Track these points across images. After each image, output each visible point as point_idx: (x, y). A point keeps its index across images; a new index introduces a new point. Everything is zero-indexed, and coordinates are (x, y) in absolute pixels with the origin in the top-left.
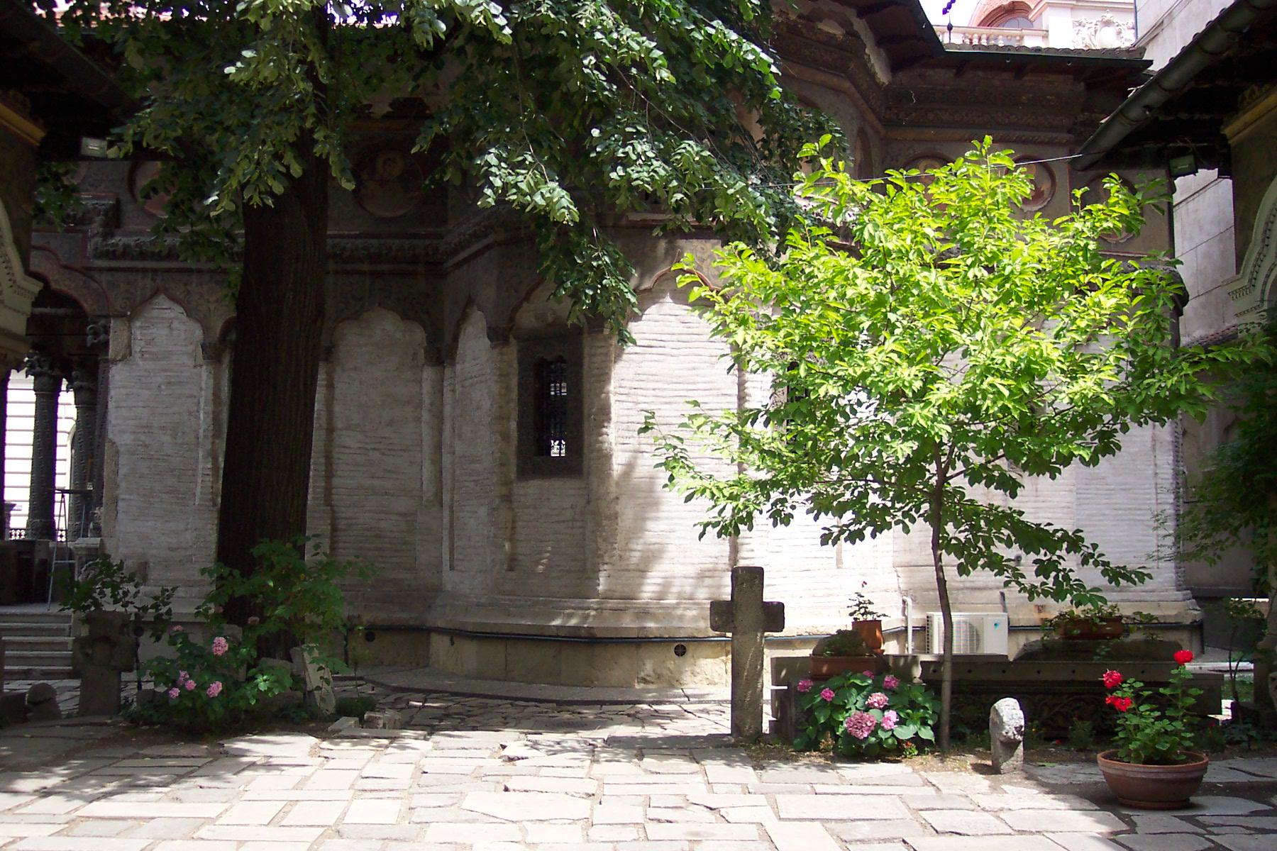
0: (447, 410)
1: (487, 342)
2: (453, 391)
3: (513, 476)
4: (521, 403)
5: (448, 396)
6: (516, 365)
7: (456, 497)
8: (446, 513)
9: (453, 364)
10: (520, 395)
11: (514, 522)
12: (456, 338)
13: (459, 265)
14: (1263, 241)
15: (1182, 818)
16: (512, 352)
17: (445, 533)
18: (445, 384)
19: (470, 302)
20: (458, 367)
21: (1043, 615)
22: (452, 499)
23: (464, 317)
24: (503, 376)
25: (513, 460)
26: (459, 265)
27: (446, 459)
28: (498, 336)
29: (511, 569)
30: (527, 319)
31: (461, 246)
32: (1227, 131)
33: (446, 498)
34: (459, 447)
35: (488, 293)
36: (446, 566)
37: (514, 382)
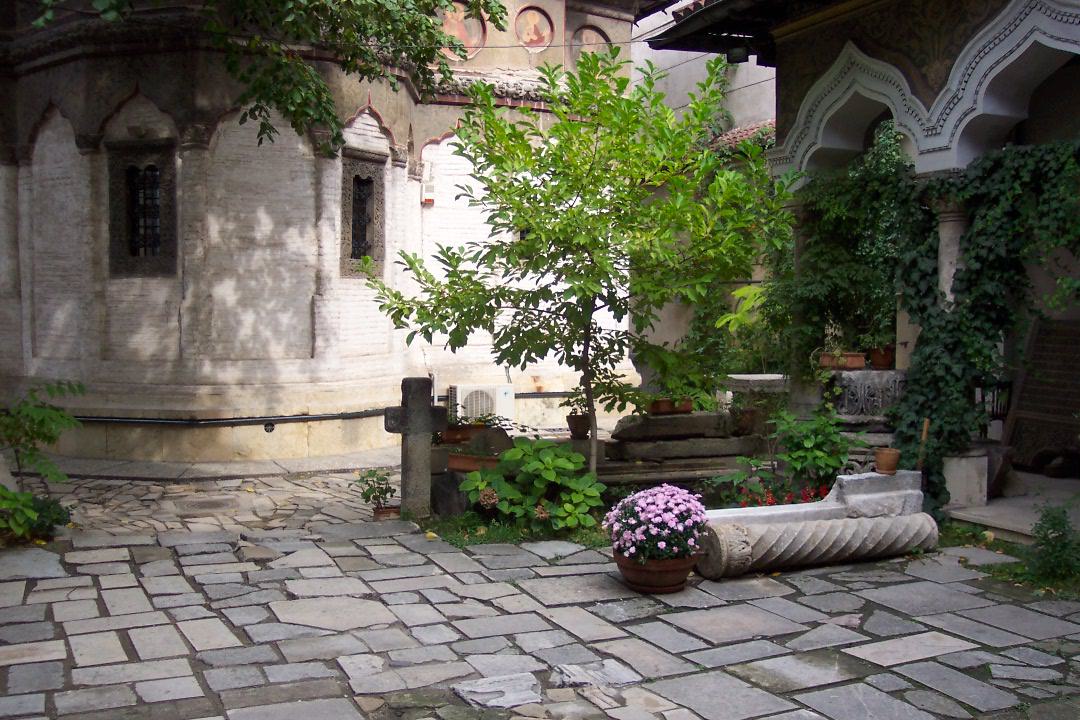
0: (24, 208)
1: (72, 146)
2: (31, 190)
3: (106, 273)
4: (113, 208)
5: (24, 195)
6: (106, 170)
7: (37, 290)
8: (26, 304)
9: (29, 164)
10: (112, 200)
11: (108, 315)
12: (33, 139)
13: (35, 70)
14: (805, 124)
15: (816, 576)
16: (104, 160)
17: (26, 323)
18: (21, 182)
19: (50, 107)
20: (35, 169)
21: (539, 384)
22: (32, 291)
23: (43, 119)
24: (94, 181)
25: (106, 260)
26: (35, 70)
27: (24, 254)
28: (89, 143)
29: (104, 359)
30: (119, 131)
31: (40, 53)
32: (775, 32)
33: (26, 290)
34: (38, 243)
35: (77, 102)
36: (28, 354)
37: (105, 188)
